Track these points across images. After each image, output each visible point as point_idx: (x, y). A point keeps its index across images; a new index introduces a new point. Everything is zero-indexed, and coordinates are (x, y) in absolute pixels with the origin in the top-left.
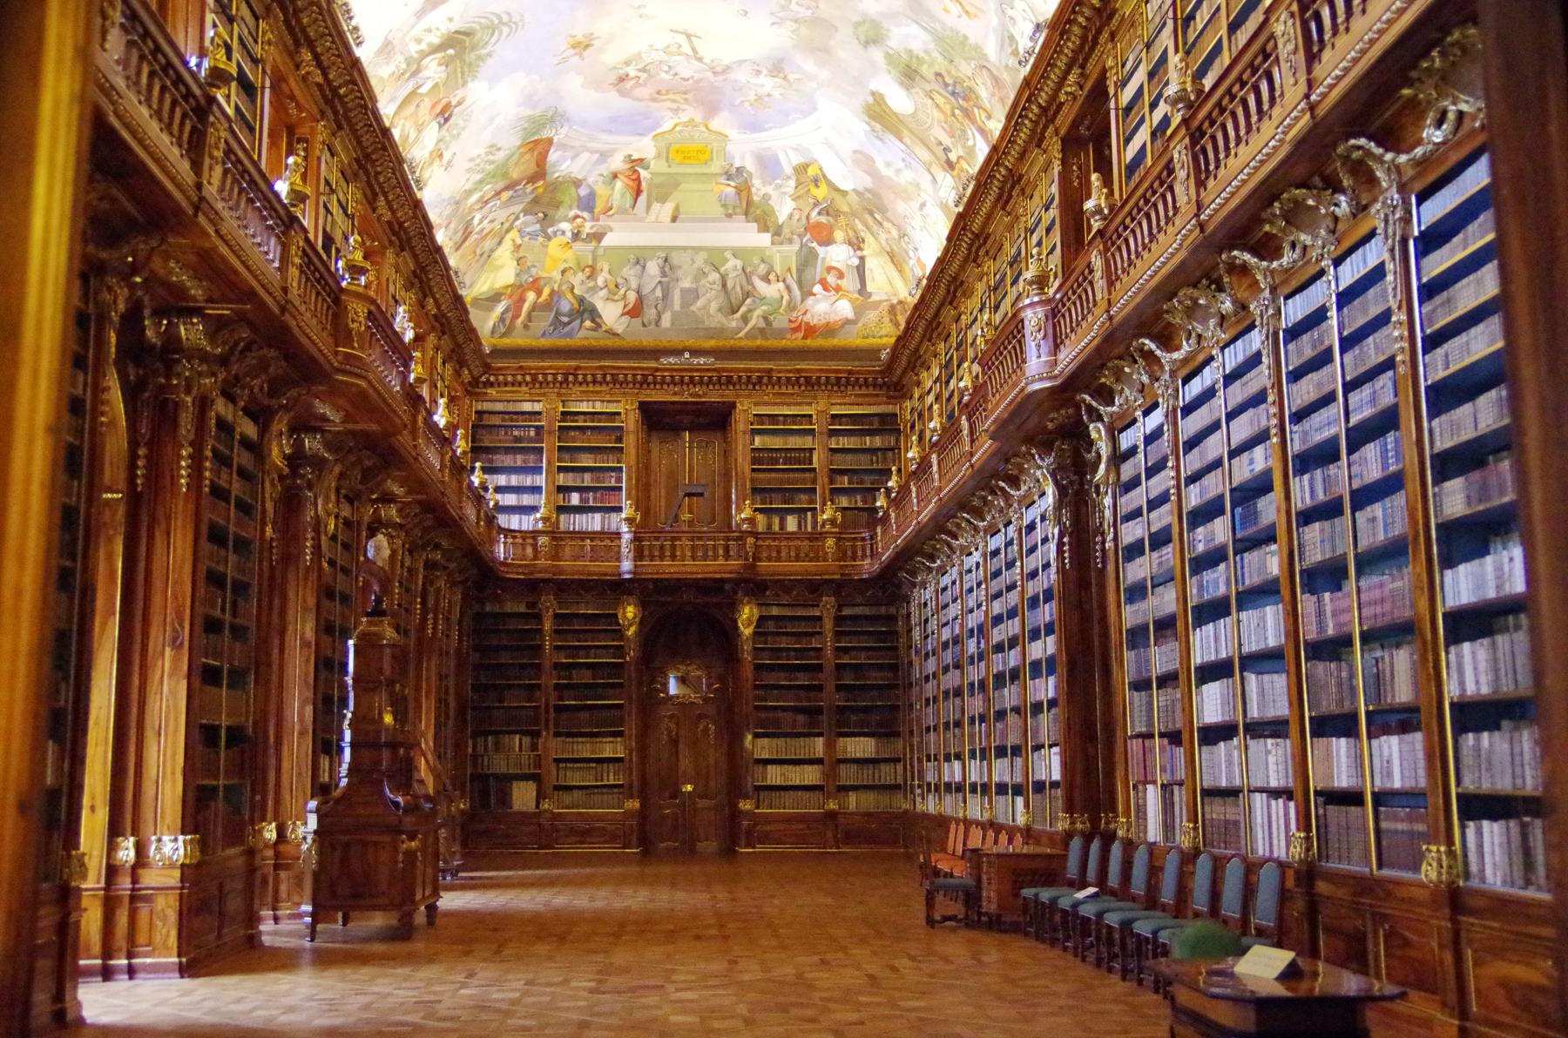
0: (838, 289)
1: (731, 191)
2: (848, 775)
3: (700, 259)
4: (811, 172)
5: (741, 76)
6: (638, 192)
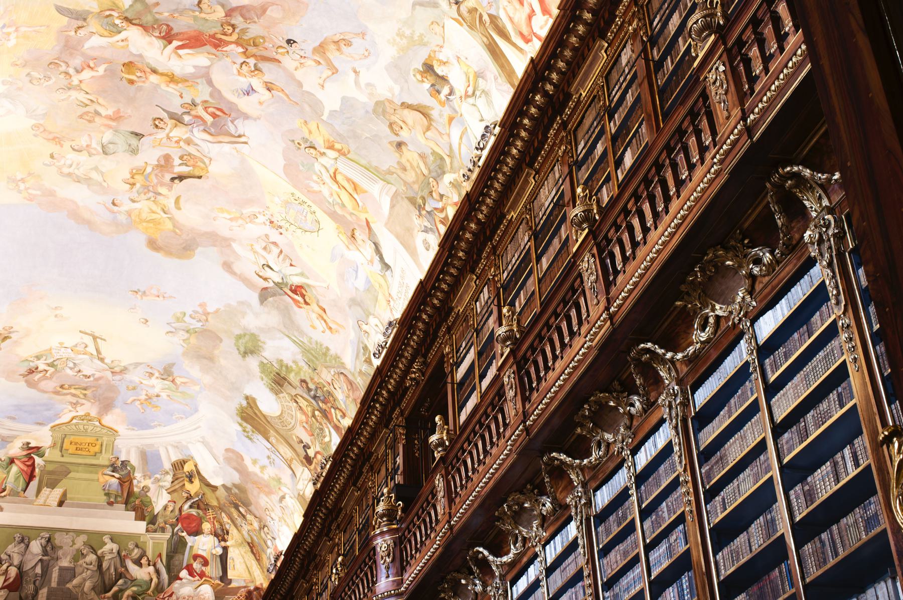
0: (202, 575)
1: (115, 481)
3: (83, 538)
4: (188, 468)
5: (134, 377)
6: (31, 477)
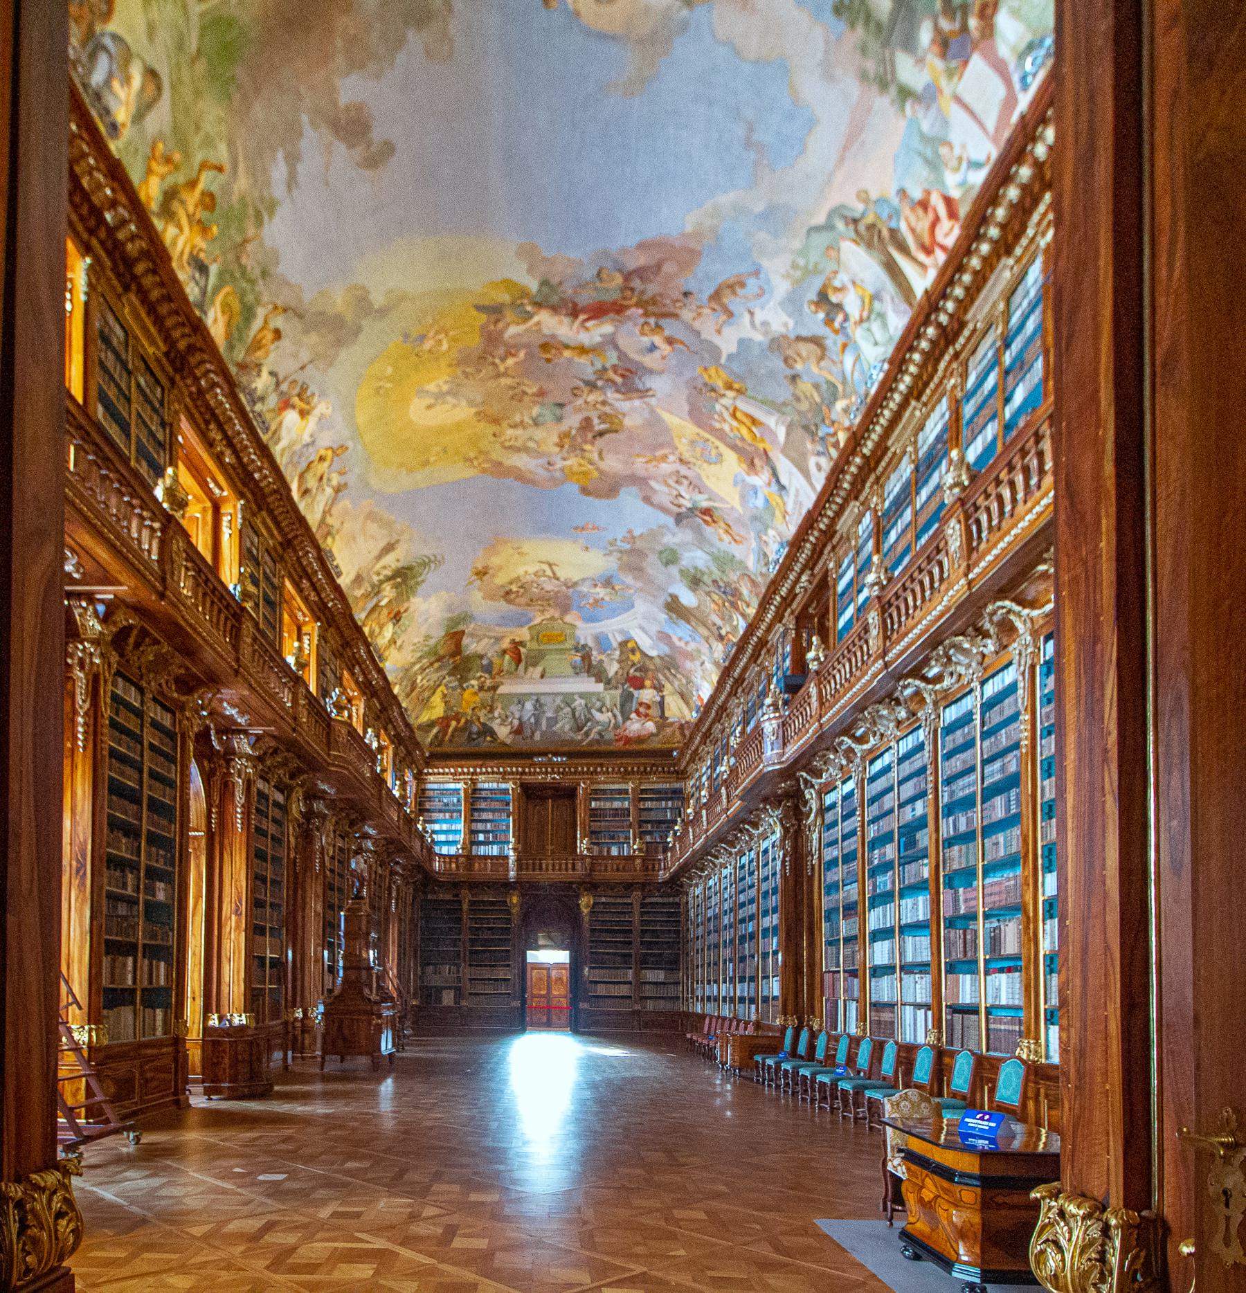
1: (578, 659)
2: (648, 991)
5: (584, 589)
